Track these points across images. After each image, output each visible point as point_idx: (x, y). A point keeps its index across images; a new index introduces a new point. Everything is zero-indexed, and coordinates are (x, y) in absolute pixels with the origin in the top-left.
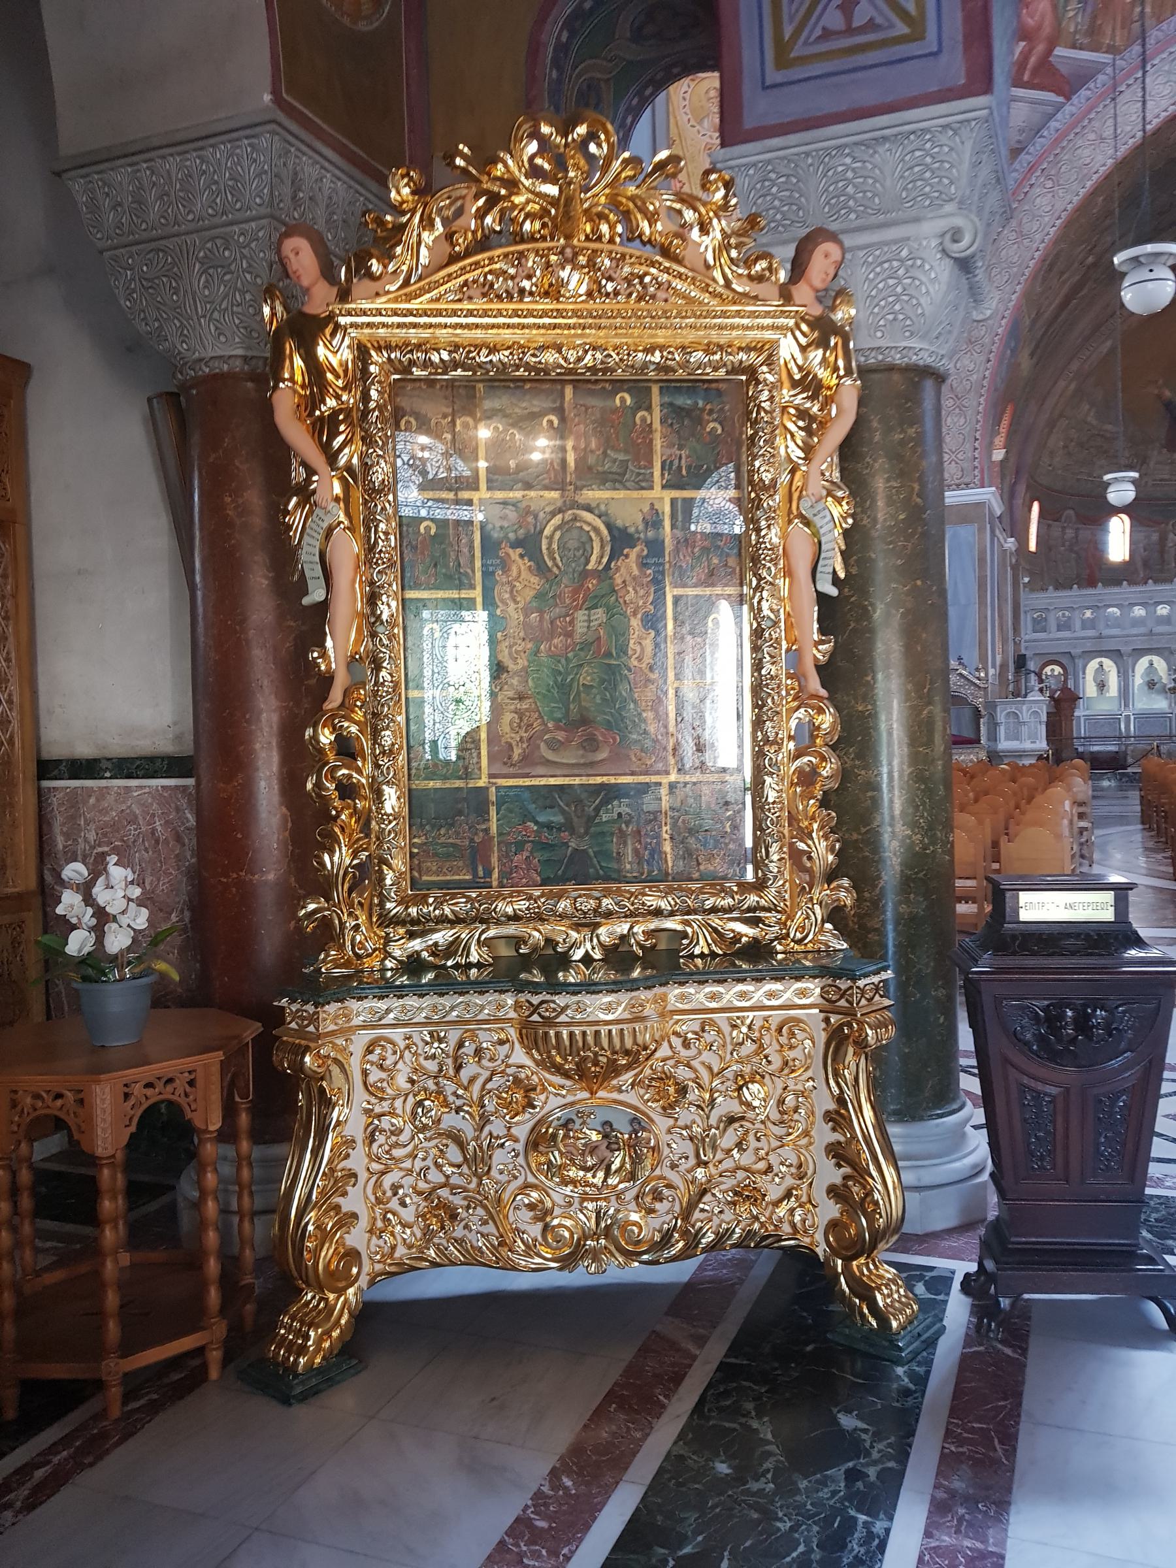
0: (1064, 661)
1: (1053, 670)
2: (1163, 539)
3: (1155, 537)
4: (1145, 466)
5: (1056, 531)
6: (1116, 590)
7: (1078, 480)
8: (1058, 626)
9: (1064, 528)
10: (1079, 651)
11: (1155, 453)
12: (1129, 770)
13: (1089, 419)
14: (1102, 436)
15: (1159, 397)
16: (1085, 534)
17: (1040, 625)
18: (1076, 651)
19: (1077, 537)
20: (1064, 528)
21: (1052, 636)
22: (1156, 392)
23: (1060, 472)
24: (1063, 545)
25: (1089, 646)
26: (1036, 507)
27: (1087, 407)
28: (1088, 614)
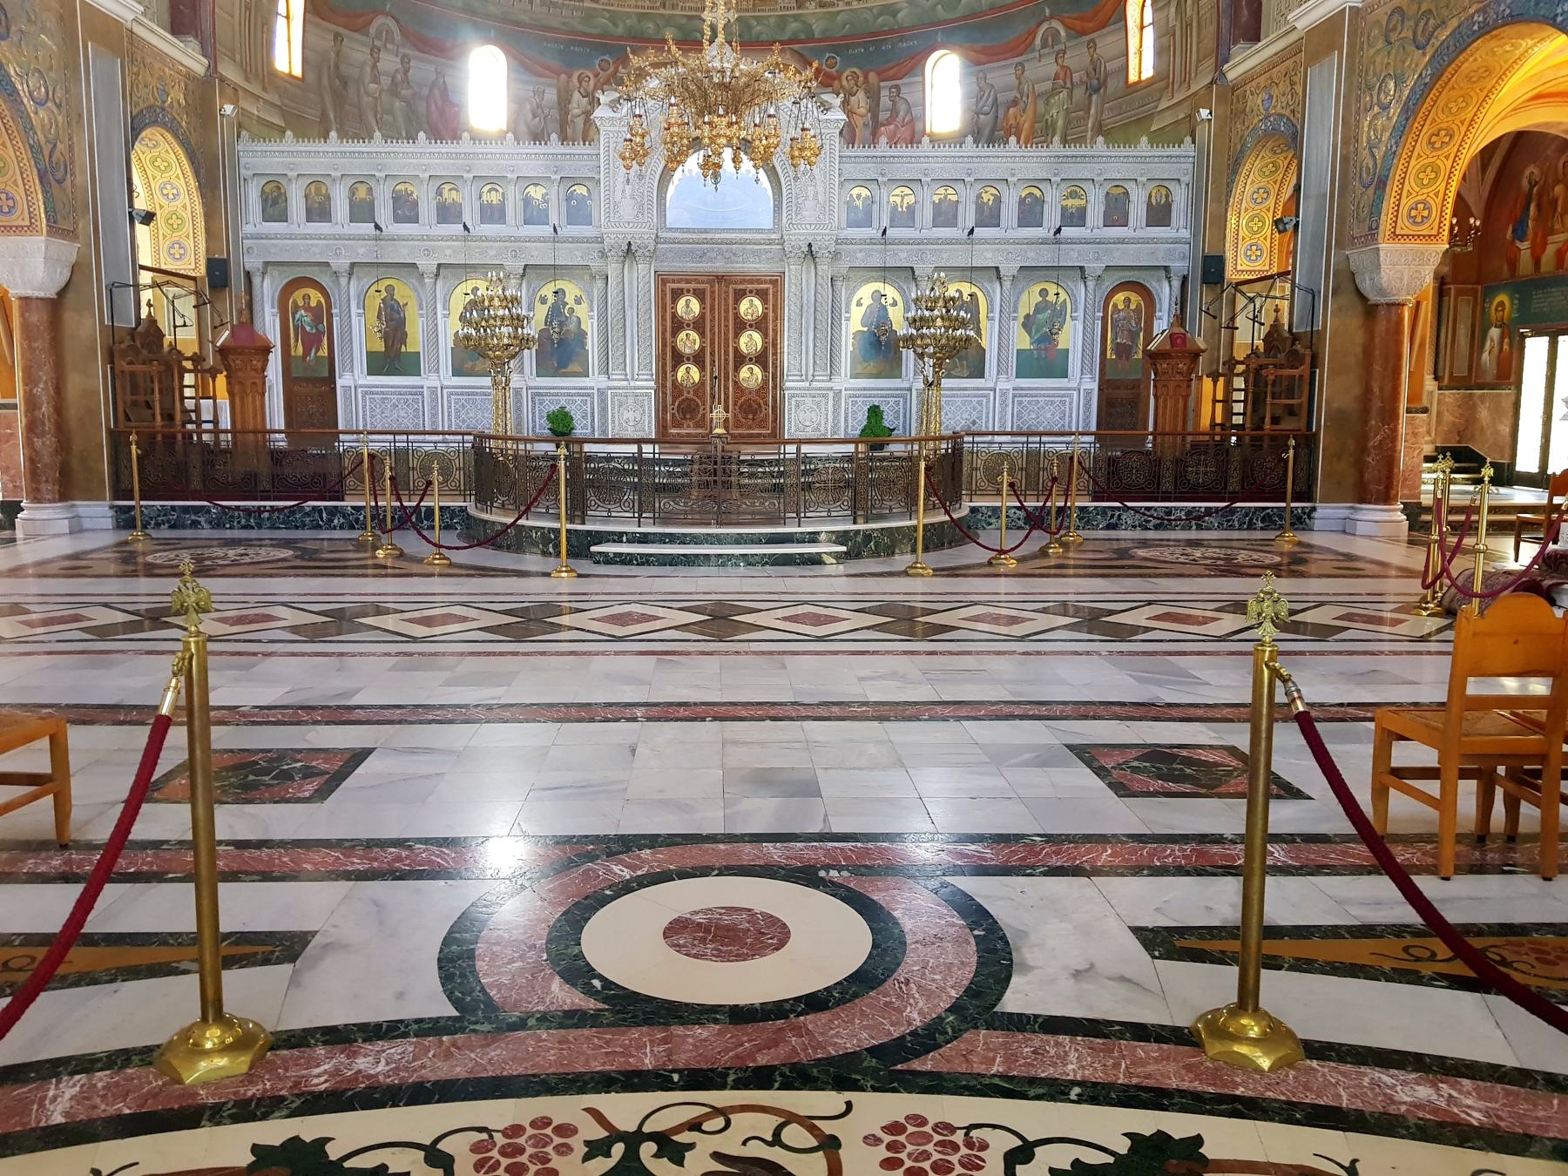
0: (325, 281)
1: (307, 297)
2: (564, 102)
3: (551, 95)
5: (357, 51)
6: (405, 147)
8: (308, 211)
9: (375, 51)
10: (341, 263)
12: (348, 503)
16: (422, 70)
17: (274, 206)
18: (341, 263)
19: (406, 72)
20: (375, 51)
21: (294, 229)
24: (376, 80)
25: (363, 253)
28: (362, 193)
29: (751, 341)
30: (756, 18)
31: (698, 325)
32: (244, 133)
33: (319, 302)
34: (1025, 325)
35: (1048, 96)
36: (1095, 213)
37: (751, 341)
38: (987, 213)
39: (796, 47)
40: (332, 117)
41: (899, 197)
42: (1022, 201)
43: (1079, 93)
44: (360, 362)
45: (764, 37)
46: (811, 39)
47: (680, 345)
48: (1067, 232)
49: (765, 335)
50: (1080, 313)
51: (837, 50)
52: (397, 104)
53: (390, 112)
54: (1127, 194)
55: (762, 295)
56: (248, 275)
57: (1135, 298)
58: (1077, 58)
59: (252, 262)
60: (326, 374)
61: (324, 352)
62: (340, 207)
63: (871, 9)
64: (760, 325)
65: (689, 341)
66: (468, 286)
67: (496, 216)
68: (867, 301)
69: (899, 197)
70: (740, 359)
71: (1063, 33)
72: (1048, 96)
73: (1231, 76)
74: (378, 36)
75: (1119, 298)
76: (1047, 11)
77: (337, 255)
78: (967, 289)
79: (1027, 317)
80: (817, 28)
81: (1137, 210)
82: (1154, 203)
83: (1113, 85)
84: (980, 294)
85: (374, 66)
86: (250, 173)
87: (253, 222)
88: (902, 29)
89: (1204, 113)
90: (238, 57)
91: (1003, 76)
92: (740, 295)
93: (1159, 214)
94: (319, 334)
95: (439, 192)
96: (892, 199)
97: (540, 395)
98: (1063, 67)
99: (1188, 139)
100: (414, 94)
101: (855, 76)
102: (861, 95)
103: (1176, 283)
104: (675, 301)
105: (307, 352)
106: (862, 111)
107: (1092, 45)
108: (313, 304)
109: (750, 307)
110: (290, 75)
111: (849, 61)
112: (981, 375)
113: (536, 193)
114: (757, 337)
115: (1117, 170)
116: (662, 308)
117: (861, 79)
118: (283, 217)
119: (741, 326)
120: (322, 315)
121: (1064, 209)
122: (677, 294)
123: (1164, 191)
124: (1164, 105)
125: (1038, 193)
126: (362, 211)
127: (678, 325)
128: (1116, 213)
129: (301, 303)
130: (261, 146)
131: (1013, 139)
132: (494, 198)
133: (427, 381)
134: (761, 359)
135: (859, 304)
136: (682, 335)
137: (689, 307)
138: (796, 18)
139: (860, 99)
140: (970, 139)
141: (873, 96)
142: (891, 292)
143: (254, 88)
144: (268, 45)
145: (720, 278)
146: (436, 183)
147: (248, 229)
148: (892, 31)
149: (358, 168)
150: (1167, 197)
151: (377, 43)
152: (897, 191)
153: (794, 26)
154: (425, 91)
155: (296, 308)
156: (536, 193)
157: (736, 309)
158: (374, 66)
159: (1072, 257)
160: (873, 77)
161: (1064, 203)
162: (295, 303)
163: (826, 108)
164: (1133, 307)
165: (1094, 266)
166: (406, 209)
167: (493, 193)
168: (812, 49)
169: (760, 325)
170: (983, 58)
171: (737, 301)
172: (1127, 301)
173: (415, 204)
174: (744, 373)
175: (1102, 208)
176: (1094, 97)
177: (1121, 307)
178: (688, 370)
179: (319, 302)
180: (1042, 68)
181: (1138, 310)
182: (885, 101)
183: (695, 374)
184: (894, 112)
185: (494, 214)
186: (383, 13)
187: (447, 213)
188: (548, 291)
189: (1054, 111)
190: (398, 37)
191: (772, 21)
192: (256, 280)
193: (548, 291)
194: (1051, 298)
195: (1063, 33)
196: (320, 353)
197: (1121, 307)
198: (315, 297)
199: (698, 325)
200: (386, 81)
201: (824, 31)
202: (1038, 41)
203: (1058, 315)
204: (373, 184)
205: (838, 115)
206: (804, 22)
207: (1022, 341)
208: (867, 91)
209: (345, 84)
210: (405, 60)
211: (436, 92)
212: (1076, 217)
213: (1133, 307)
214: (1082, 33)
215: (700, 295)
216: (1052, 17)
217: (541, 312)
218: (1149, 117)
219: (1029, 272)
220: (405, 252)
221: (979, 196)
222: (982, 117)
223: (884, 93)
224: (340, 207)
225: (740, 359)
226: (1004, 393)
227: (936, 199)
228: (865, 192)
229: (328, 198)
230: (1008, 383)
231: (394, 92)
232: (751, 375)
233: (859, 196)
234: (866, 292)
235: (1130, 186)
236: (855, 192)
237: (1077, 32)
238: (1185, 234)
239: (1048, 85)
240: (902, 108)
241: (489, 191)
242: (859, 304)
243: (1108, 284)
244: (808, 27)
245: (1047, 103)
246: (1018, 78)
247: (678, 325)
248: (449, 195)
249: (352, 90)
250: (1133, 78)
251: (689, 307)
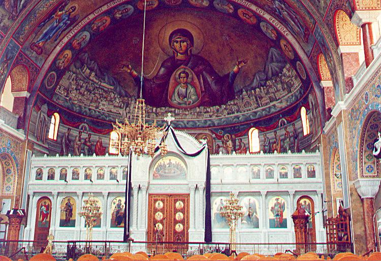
0: (51, 198)
1: (45, 202)
4: (128, 109)
5: (75, 133)
7: (90, 109)
8: (48, 177)
9: (80, 132)
11: (133, 102)
13: (91, 78)
14: (102, 89)
15: (131, 74)
19: (89, 138)
22: (129, 71)
23: (76, 102)
24: (80, 140)
27: (88, 71)
28: (64, 172)
29: (179, 216)
30: (198, 121)
31: (162, 210)
32: (34, 155)
33: (49, 204)
34: (271, 210)
35: (283, 140)
36: (291, 174)
37: (179, 216)
38: (256, 174)
39: (210, 128)
40: (64, 151)
42: (267, 171)
43: (292, 139)
44: (58, 222)
45: (200, 126)
46: (214, 126)
47: (156, 217)
48: (281, 180)
49: (184, 214)
50: (289, 207)
51: (222, 129)
52: (86, 147)
53: (83, 149)
54: (300, 168)
55: (183, 201)
56: (29, 196)
57: (308, 201)
58: (290, 129)
59: (31, 192)
60: (48, 226)
61: (48, 220)
62: (57, 176)
63: (231, 117)
64: (183, 210)
65: (159, 216)
67: (102, 178)
70: (176, 222)
71: (286, 122)
72: (283, 140)
73: (326, 132)
74: (82, 129)
75: (302, 201)
76: (281, 116)
77: (54, 190)
79: (272, 208)
80: (216, 123)
81: (304, 173)
82: (309, 170)
83: (300, 136)
85: (80, 137)
86: (34, 166)
87: (33, 180)
88: (241, 122)
90: (36, 135)
91: (271, 135)
92: (176, 201)
93: (312, 174)
94: (47, 214)
95: (86, 171)
97: (111, 233)
98: (287, 132)
99: (317, 151)
100: (92, 145)
101: (228, 136)
102: (230, 142)
103: (320, 196)
104: (155, 203)
105: (43, 219)
106: (231, 146)
107: (294, 125)
108: (47, 205)
109: (179, 205)
110: (53, 140)
111: (228, 132)
112: (258, 227)
114: (182, 215)
115: (296, 161)
116: (150, 205)
117: (230, 137)
118: (41, 179)
119: (176, 211)
120: (48, 208)
121: (281, 173)
122: (156, 201)
123: (312, 167)
124: (313, 141)
125: (272, 168)
126: (63, 177)
127: (156, 210)
128: (297, 173)
129: (43, 204)
130: (38, 158)
131: (275, 151)
132: (102, 172)
133: (76, 228)
134: (182, 222)
136: (157, 214)
137: (160, 205)
138: (209, 120)
139: (230, 143)
140: (262, 152)
141: (234, 142)
143: (40, 143)
144: (48, 131)
145: (171, 195)
146: (85, 168)
147: (31, 182)
148: (238, 123)
149: (63, 164)
150: (314, 168)
151: (82, 131)
153: (209, 122)
154: (95, 143)
155: (42, 206)
156: (114, 171)
157: (175, 205)
158: (80, 137)
159: (283, 188)
160: (233, 136)
161: (280, 171)
162: (42, 204)
164: (307, 204)
165: (292, 191)
166: (76, 176)
168: (215, 129)
169: (183, 210)
170: (265, 130)
171: (175, 203)
172: (305, 202)
173: (79, 174)
174: (177, 226)
175: (293, 172)
176: (296, 140)
177: (303, 204)
178: (158, 226)
179: (49, 204)
180: (281, 132)
181: (309, 205)
182: (237, 143)
183: (161, 226)
184: (240, 146)
185: (100, 177)
186: (85, 123)
187: (87, 177)
189: (286, 145)
190: (88, 129)
191: (203, 121)
192: (31, 197)
194: (279, 201)
195: (286, 122)
196: (47, 220)
197: (303, 204)
198: (48, 202)
199: (162, 210)
200: (83, 141)
201: (218, 123)
202: (279, 124)
203: (282, 207)
204: (67, 168)
206: (212, 121)
207: (272, 216)
208: (232, 141)
209: (70, 142)
210: (90, 135)
211: (99, 144)
212: (285, 176)
213: (307, 204)
214: (291, 121)
215: (163, 201)
216: (283, 117)
217: (114, 206)
218: (310, 145)
219: (268, 193)
220: (73, 188)
221: (253, 169)
222: (266, 147)
223: (237, 141)
224: (57, 176)
225: (176, 222)
226: (265, 233)
229: (54, 173)
230: (265, 230)
231: (85, 144)
232: (179, 227)
235: (301, 166)
237: (289, 122)
238: (321, 180)
239: (283, 137)
240: (243, 145)
242: (216, 204)
243: (298, 197)
244: (213, 123)
245: (284, 142)
246: (275, 135)
247: (156, 210)
248: (88, 172)
249: (72, 143)
251: (160, 205)
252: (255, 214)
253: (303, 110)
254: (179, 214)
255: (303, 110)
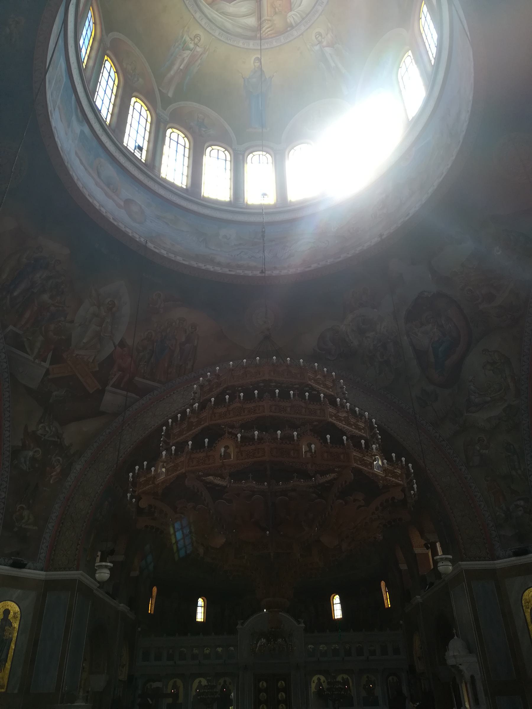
26: (155, 589)
41: (323, 647)
66: (197, 681)
68: (316, 681)
69: (323, 647)
75: (390, 678)
78: (345, 676)
84: (349, 678)
89: (401, 622)
96: (320, 648)
113: (219, 650)
135: (314, 682)
137: (263, 684)
142: (322, 678)
152: (321, 646)
163: (299, 623)
167: (207, 650)
188: (221, 681)
193: (221, 681)
205: (303, 625)
227: (333, 648)
228: (312, 646)
233: (311, 648)
234: (315, 678)
236: (310, 646)
241: (206, 650)
250: (386, 606)
252: (349, 692)
253: (383, 584)
254: (281, 694)
255: (383, 584)
